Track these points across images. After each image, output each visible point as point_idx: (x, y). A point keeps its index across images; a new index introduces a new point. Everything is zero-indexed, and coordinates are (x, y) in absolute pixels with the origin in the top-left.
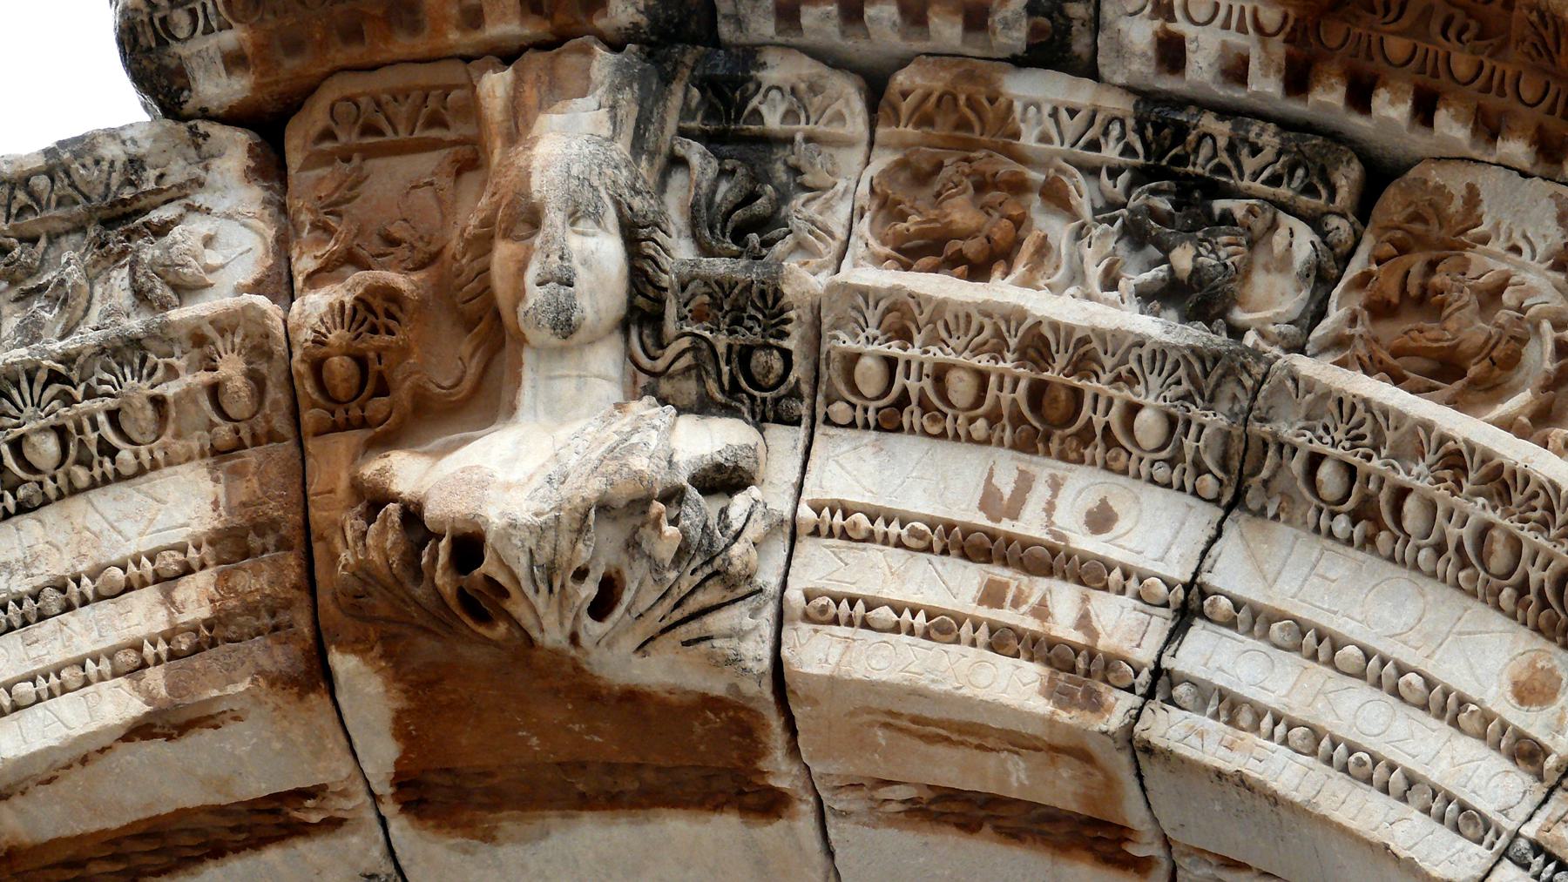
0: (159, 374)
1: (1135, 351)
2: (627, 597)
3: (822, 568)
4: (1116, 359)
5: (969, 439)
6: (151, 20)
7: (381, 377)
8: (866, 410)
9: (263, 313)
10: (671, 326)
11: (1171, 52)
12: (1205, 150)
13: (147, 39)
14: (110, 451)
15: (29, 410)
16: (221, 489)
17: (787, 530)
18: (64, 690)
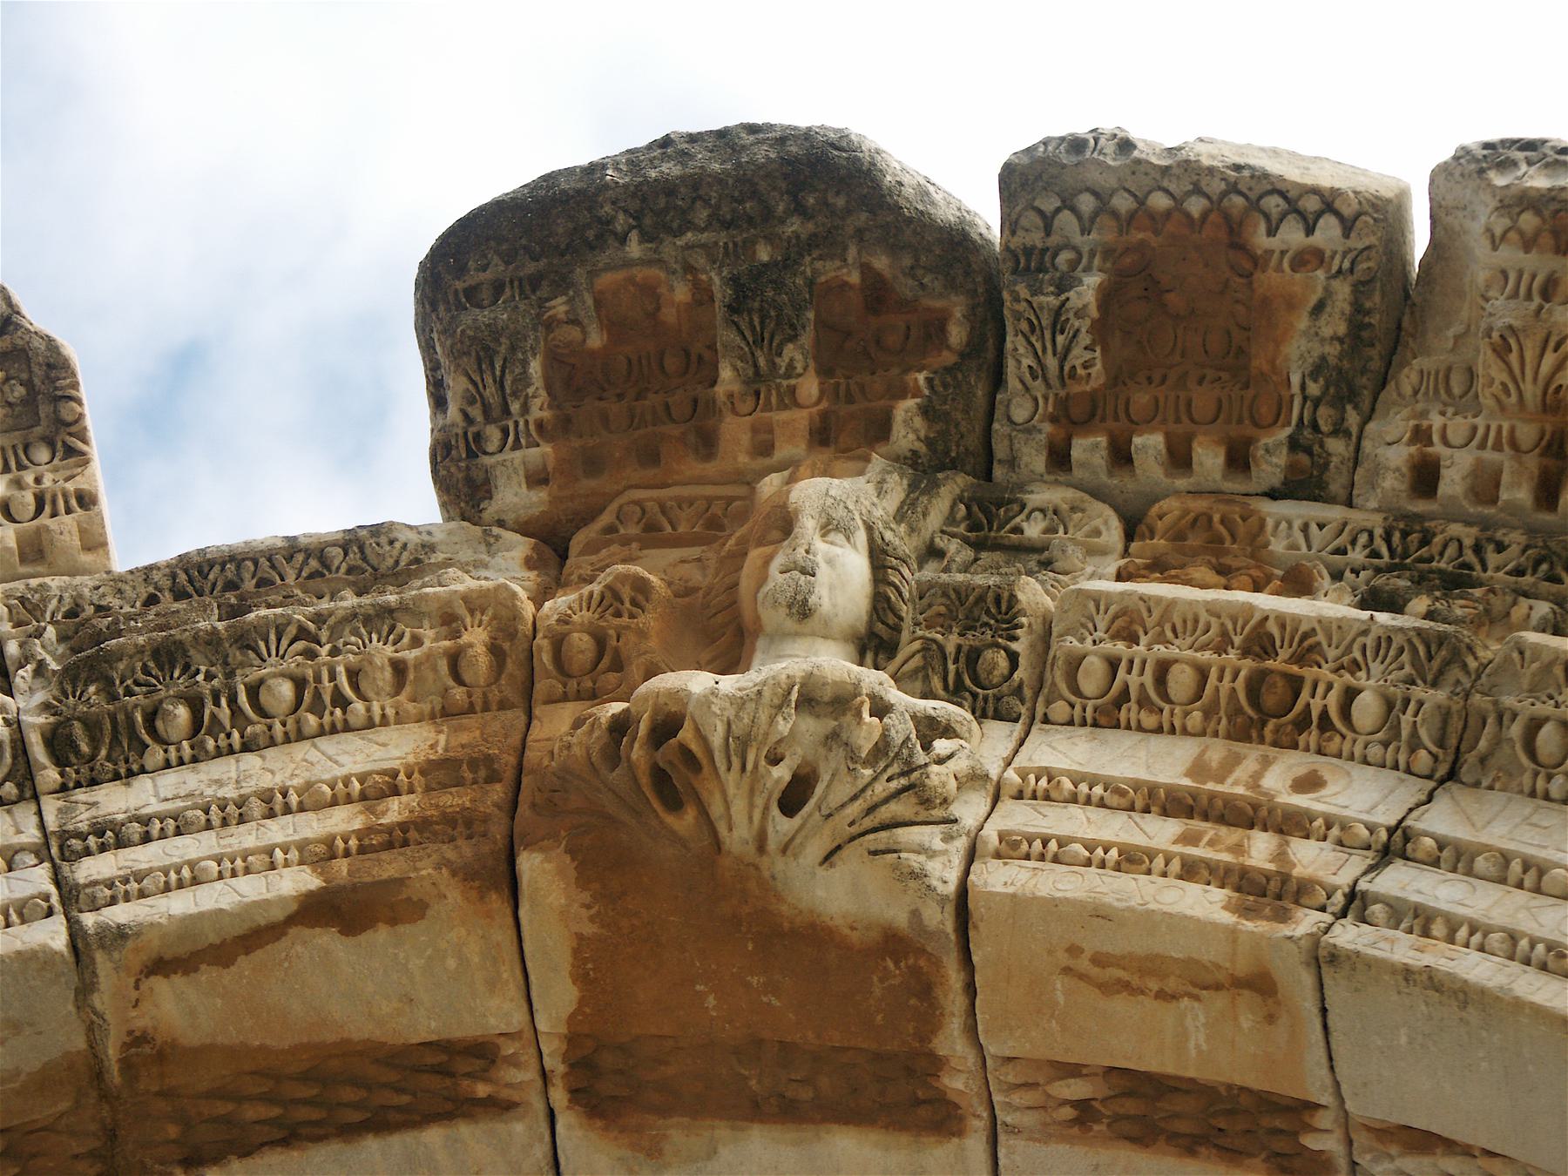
0: (406, 640)
1: (1361, 640)
2: (819, 790)
4: (1338, 652)
6: (466, 434)
7: (617, 651)
11: (1425, 477)
12: (1451, 550)
14: (341, 701)
15: (274, 659)
17: (991, 788)
18: (247, 871)
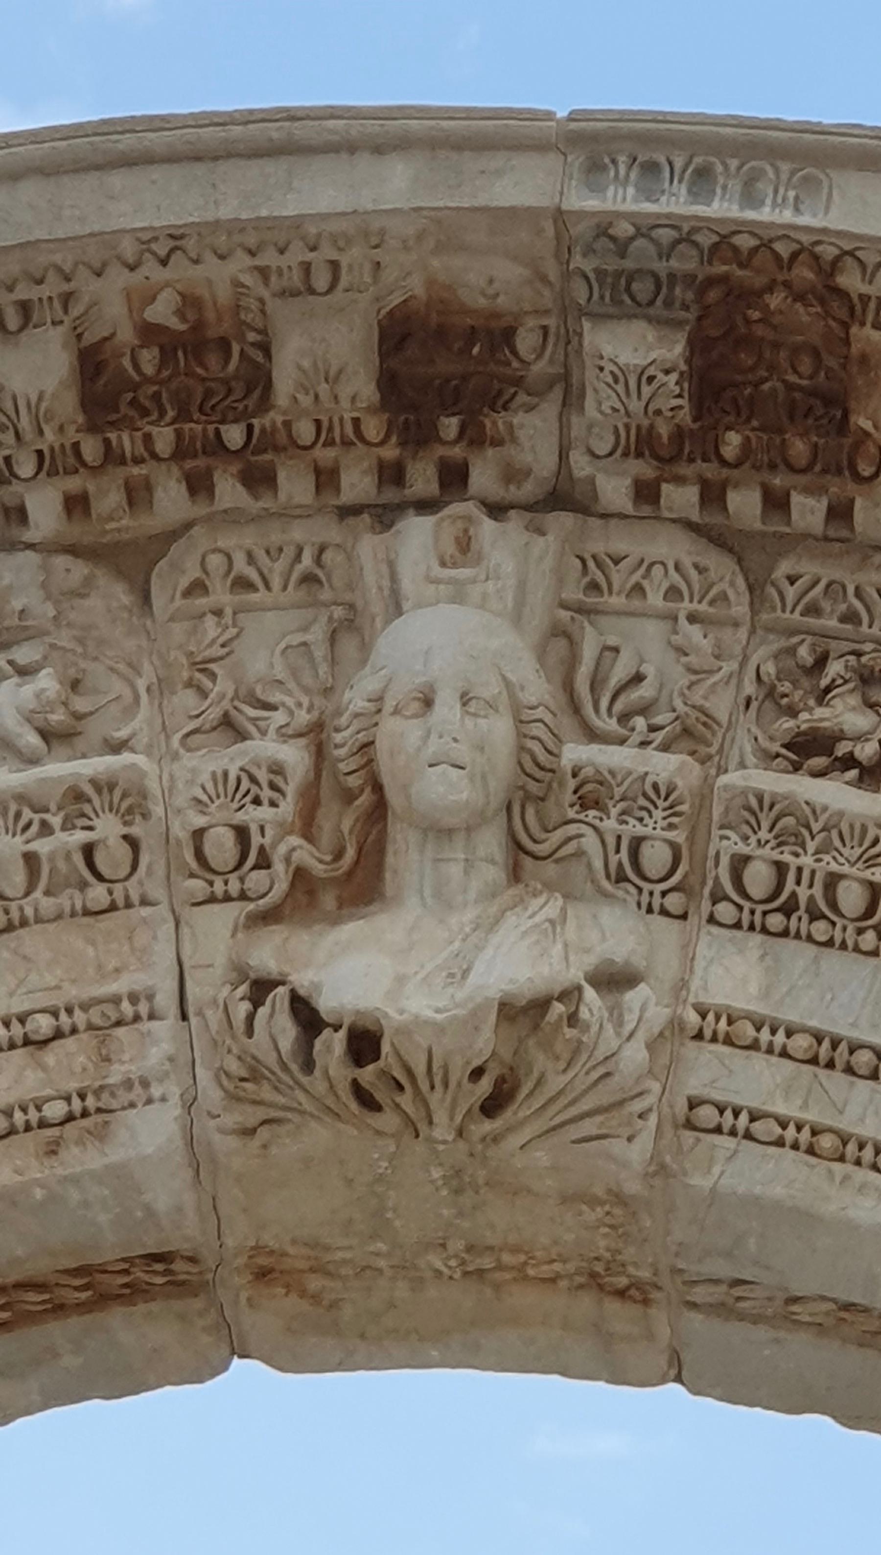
0: (35, 828)
5: (857, 949)
8: (752, 912)
9: (143, 774)
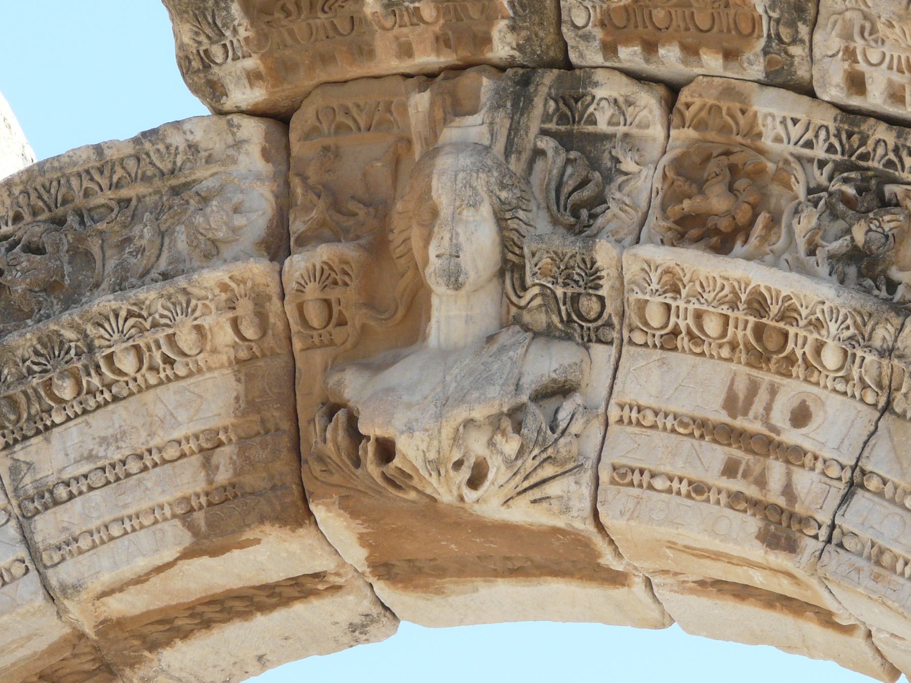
2: (491, 476)
3: (626, 447)
4: (808, 311)
6: (198, 51)
7: (340, 312)
8: (654, 336)
10: (529, 280)
12: (880, 151)
13: (196, 64)
14: (168, 361)
15: (116, 336)
16: (241, 388)
